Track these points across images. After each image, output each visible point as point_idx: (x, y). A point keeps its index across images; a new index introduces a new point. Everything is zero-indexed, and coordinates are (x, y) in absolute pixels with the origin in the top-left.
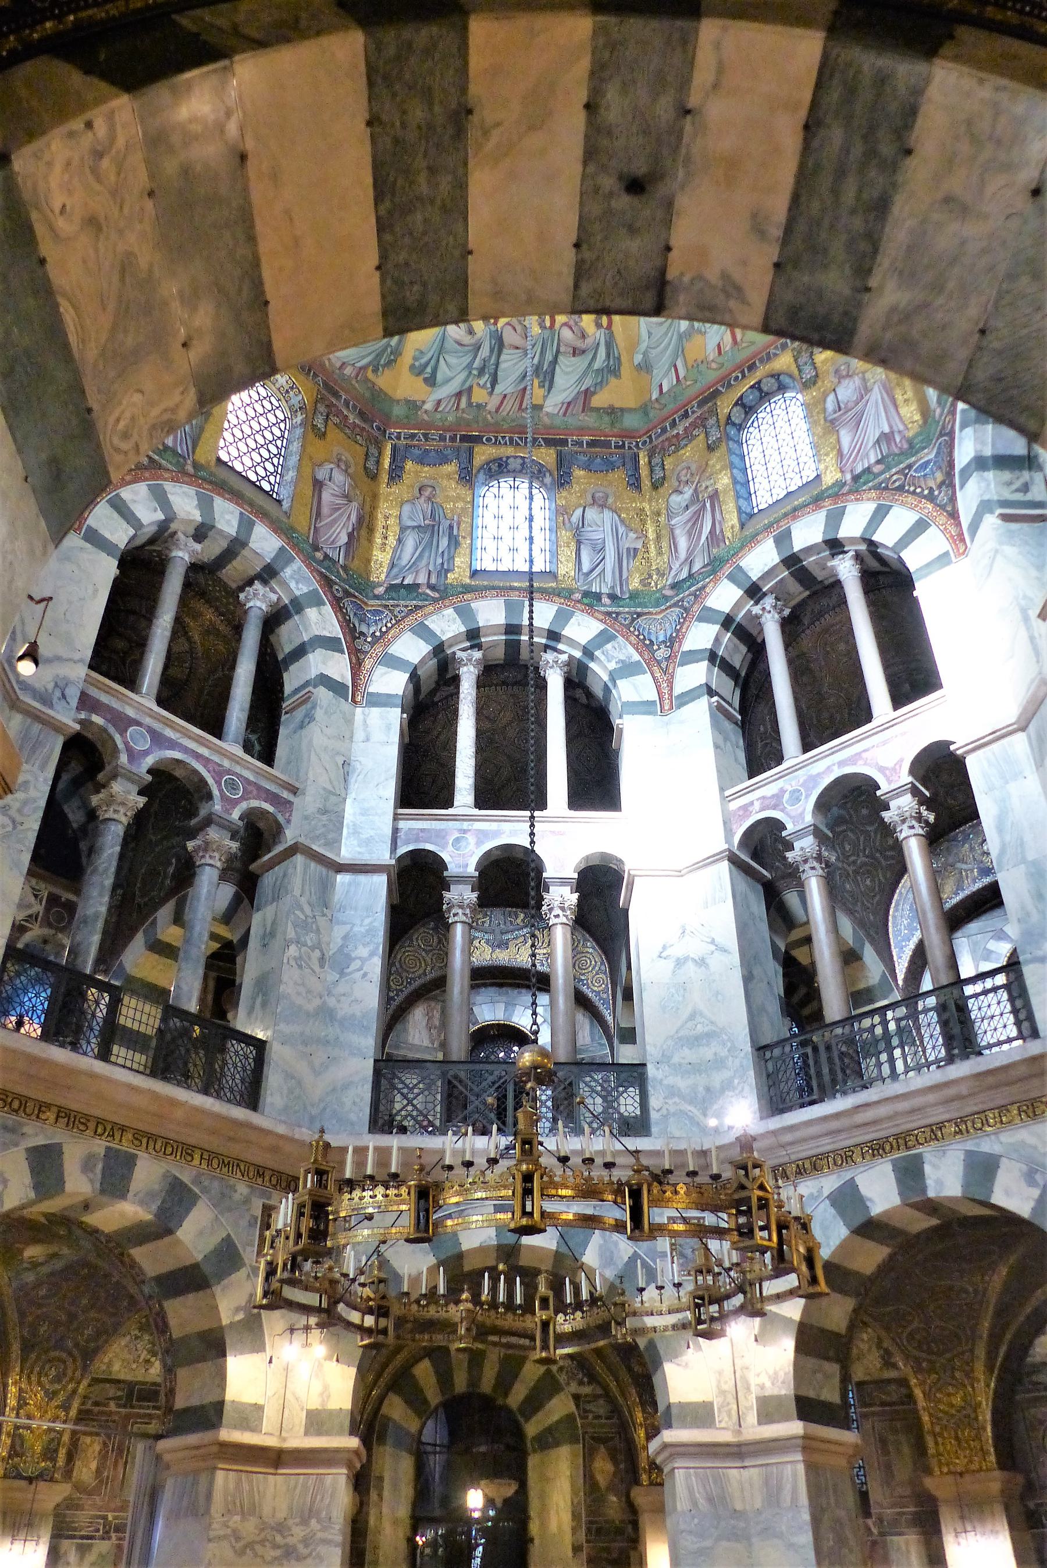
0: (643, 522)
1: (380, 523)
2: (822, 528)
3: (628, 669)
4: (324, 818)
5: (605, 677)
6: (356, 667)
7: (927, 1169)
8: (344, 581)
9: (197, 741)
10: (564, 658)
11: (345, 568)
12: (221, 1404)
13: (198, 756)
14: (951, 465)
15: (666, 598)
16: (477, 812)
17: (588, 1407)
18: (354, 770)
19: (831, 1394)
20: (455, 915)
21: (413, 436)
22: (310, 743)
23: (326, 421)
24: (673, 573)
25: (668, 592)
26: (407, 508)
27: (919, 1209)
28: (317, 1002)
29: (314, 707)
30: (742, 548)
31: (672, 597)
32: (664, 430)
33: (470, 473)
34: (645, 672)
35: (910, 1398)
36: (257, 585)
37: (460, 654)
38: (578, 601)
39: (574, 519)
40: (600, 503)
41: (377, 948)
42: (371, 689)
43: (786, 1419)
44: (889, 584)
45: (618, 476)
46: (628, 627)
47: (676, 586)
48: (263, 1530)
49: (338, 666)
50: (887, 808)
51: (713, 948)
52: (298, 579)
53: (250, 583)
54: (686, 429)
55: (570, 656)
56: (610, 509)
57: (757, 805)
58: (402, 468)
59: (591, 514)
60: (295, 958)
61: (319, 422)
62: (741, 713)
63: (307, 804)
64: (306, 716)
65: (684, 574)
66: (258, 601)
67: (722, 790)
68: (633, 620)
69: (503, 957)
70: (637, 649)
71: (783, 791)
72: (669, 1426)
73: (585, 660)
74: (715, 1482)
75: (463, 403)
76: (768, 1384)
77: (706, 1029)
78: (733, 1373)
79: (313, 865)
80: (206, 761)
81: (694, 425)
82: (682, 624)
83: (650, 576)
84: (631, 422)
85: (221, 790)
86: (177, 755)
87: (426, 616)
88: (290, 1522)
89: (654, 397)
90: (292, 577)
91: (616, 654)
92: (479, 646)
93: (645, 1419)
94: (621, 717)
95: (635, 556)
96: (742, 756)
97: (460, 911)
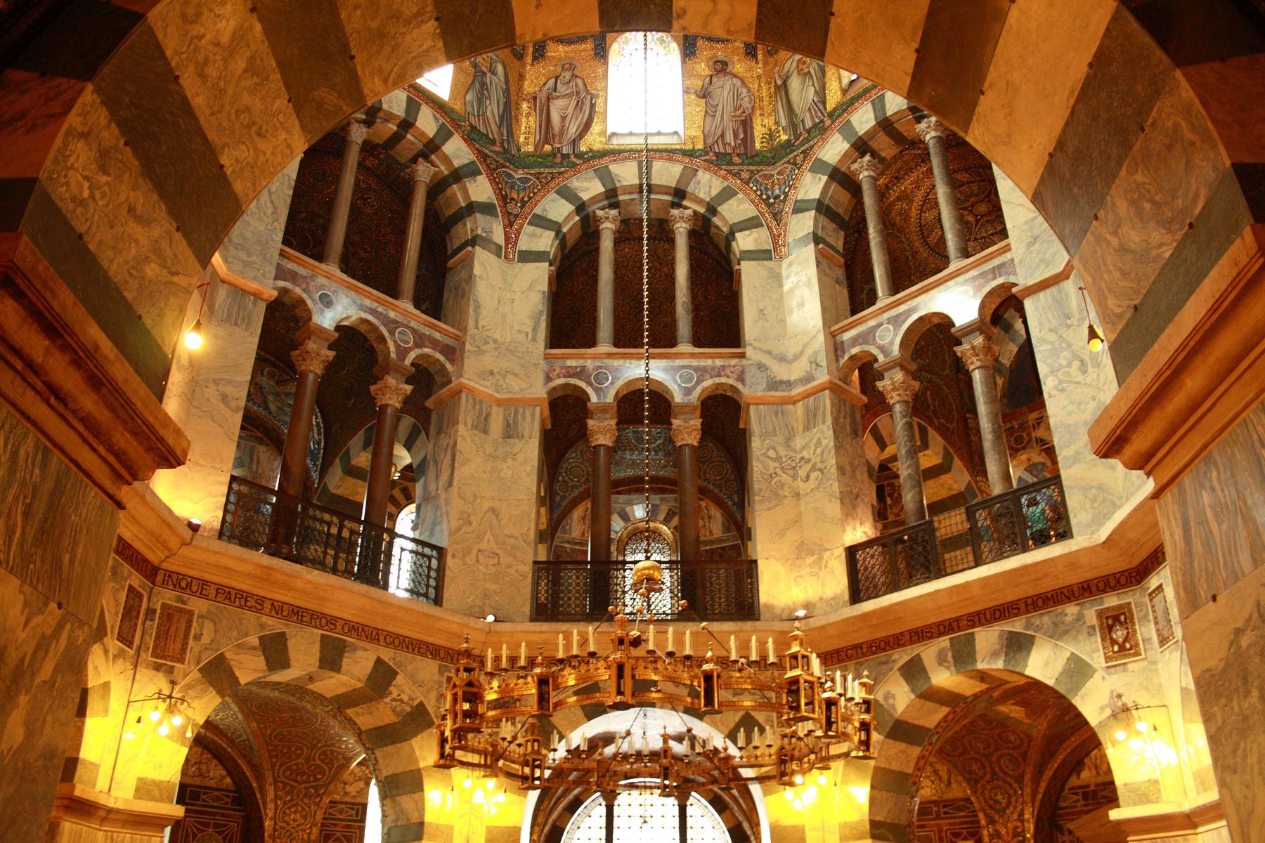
4: (1036, 247)
60: (1055, 388)
79: (1041, 295)
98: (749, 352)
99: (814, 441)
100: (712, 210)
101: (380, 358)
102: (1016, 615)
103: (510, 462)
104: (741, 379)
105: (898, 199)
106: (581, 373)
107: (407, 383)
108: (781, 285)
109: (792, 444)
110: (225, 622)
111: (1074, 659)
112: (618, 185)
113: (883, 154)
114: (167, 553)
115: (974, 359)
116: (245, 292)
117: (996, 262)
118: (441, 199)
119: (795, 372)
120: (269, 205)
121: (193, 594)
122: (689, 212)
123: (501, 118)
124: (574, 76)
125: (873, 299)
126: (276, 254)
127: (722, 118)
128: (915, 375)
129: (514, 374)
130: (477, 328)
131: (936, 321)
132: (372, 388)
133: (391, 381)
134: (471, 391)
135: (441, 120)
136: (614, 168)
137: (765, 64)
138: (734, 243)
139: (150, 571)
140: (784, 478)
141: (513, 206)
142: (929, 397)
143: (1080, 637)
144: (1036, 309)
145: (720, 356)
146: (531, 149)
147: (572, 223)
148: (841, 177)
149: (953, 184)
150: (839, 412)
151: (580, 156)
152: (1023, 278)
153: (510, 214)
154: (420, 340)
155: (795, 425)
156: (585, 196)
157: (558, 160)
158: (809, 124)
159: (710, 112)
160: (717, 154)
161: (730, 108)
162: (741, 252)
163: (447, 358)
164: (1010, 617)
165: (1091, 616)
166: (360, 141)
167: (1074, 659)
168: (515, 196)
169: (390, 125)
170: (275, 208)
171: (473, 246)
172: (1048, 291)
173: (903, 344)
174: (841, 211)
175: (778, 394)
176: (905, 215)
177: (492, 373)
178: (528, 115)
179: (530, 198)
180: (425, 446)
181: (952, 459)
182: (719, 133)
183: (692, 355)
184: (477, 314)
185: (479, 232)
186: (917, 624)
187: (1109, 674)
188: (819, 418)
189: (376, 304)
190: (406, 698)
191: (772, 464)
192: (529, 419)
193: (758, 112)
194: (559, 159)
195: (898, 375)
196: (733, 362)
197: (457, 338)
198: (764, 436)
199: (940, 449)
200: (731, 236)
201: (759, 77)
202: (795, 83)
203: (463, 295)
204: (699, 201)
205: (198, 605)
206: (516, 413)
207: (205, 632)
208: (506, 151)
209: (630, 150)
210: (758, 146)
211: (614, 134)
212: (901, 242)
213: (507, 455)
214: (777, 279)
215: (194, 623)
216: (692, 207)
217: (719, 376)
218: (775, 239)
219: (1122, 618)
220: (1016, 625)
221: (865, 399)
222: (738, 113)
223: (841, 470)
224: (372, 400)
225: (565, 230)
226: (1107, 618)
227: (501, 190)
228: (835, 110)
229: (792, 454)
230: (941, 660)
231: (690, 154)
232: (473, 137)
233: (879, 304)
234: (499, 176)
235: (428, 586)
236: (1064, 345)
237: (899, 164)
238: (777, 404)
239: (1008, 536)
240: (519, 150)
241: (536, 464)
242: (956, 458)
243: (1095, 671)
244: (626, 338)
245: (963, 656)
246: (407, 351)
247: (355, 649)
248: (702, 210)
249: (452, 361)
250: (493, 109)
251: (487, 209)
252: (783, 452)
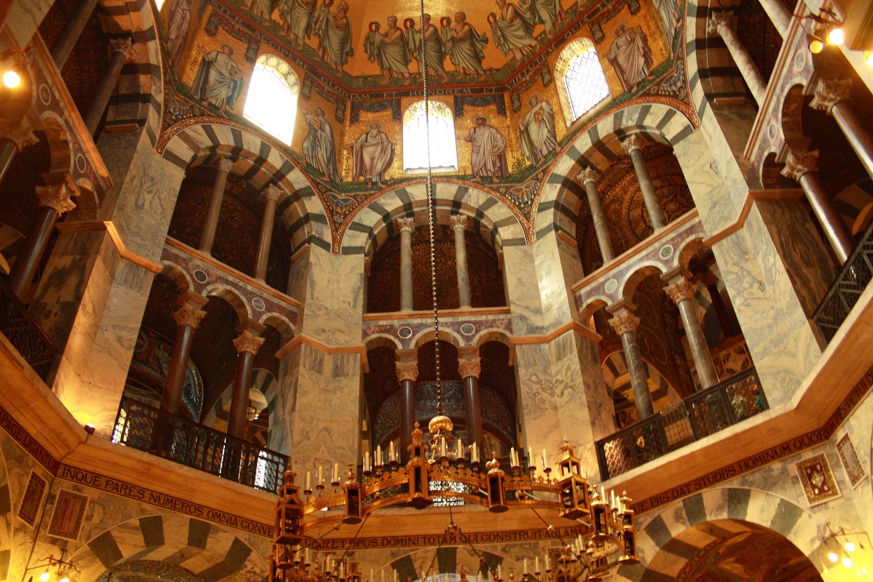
4: (717, 209)
11: (651, 73)
28: (772, 313)
60: (743, 304)
79: (724, 241)
80: (641, 260)
90: (627, 121)
98: (513, 308)
99: (565, 367)
100: (480, 214)
101: (241, 320)
102: (733, 475)
103: (338, 393)
104: (509, 327)
105: (612, 202)
106: (390, 329)
107: (261, 336)
108: (533, 262)
109: (549, 371)
110: (112, 507)
111: (784, 503)
112: (412, 200)
113: (599, 167)
114: (67, 451)
115: (679, 295)
116: (138, 265)
117: (688, 225)
118: (286, 213)
119: (547, 320)
120: (159, 207)
121: (87, 484)
122: (464, 217)
123: (329, 160)
124: (379, 132)
125: (599, 262)
126: (163, 242)
127: (484, 154)
128: (636, 313)
129: (340, 331)
130: (312, 298)
131: (648, 273)
132: (235, 341)
133: (248, 334)
134: (308, 342)
135: (286, 158)
136: (409, 189)
137: (512, 118)
138: (497, 236)
139: (54, 466)
140: (545, 395)
141: (339, 217)
142: (646, 342)
143: (787, 486)
144: (722, 251)
145: (491, 313)
146: (350, 179)
147: (380, 228)
148: (570, 185)
149: (650, 179)
150: (582, 346)
151: (385, 183)
152: (709, 232)
153: (335, 223)
154: (270, 307)
155: (550, 357)
156: (389, 209)
157: (370, 186)
158: (545, 152)
159: (475, 150)
160: (481, 177)
161: (489, 147)
162: (503, 241)
163: (291, 320)
165: (793, 468)
166: (228, 171)
167: (784, 503)
168: (339, 210)
169: (249, 161)
170: (164, 209)
171: (309, 243)
172: (729, 238)
173: (625, 292)
174: (572, 209)
175: (536, 336)
176: (618, 213)
177: (324, 331)
178: (348, 158)
179: (350, 212)
180: (276, 387)
181: (667, 386)
182: (483, 164)
183: (471, 313)
184: (312, 289)
185: (314, 233)
186: (656, 492)
187: (814, 512)
188: (568, 350)
189: (237, 280)
190: (258, 571)
191: (535, 386)
192: (352, 362)
193: (509, 149)
194: (370, 186)
195: (624, 313)
196: (502, 317)
197: (298, 306)
198: (528, 366)
199: (658, 379)
200: (495, 231)
201: (508, 127)
202: (533, 128)
203: (302, 277)
204: (471, 209)
205: (90, 493)
206: (343, 358)
207: (95, 514)
208: (332, 181)
209: (421, 177)
210: (510, 170)
211: (408, 169)
212: (617, 233)
213: (336, 388)
214: (530, 258)
215: (87, 507)
216: (465, 213)
217: (492, 326)
218: (526, 231)
219: (818, 467)
220: (735, 483)
221: (600, 337)
222: (495, 150)
223: (587, 386)
224: (234, 349)
225: (375, 232)
226: (806, 469)
227: (329, 206)
228: (562, 140)
229: (549, 378)
230: (678, 518)
231: (463, 178)
232: (308, 170)
233: (606, 266)
234: (328, 196)
235: (276, 485)
236: (745, 273)
237: (611, 175)
238: (536, 344)
239: (719, 418)
240: (342, 180)
241: (358, 394)
242: (670, 386)
243: (802, 511)
244: (421, 303)
245: (695, 511)
246: (261, 314)
247: (217, 531)
248: (473, 215)
249: (294, 323)
250: (323, 154)
251: (319, 218)
252: (542, 377)
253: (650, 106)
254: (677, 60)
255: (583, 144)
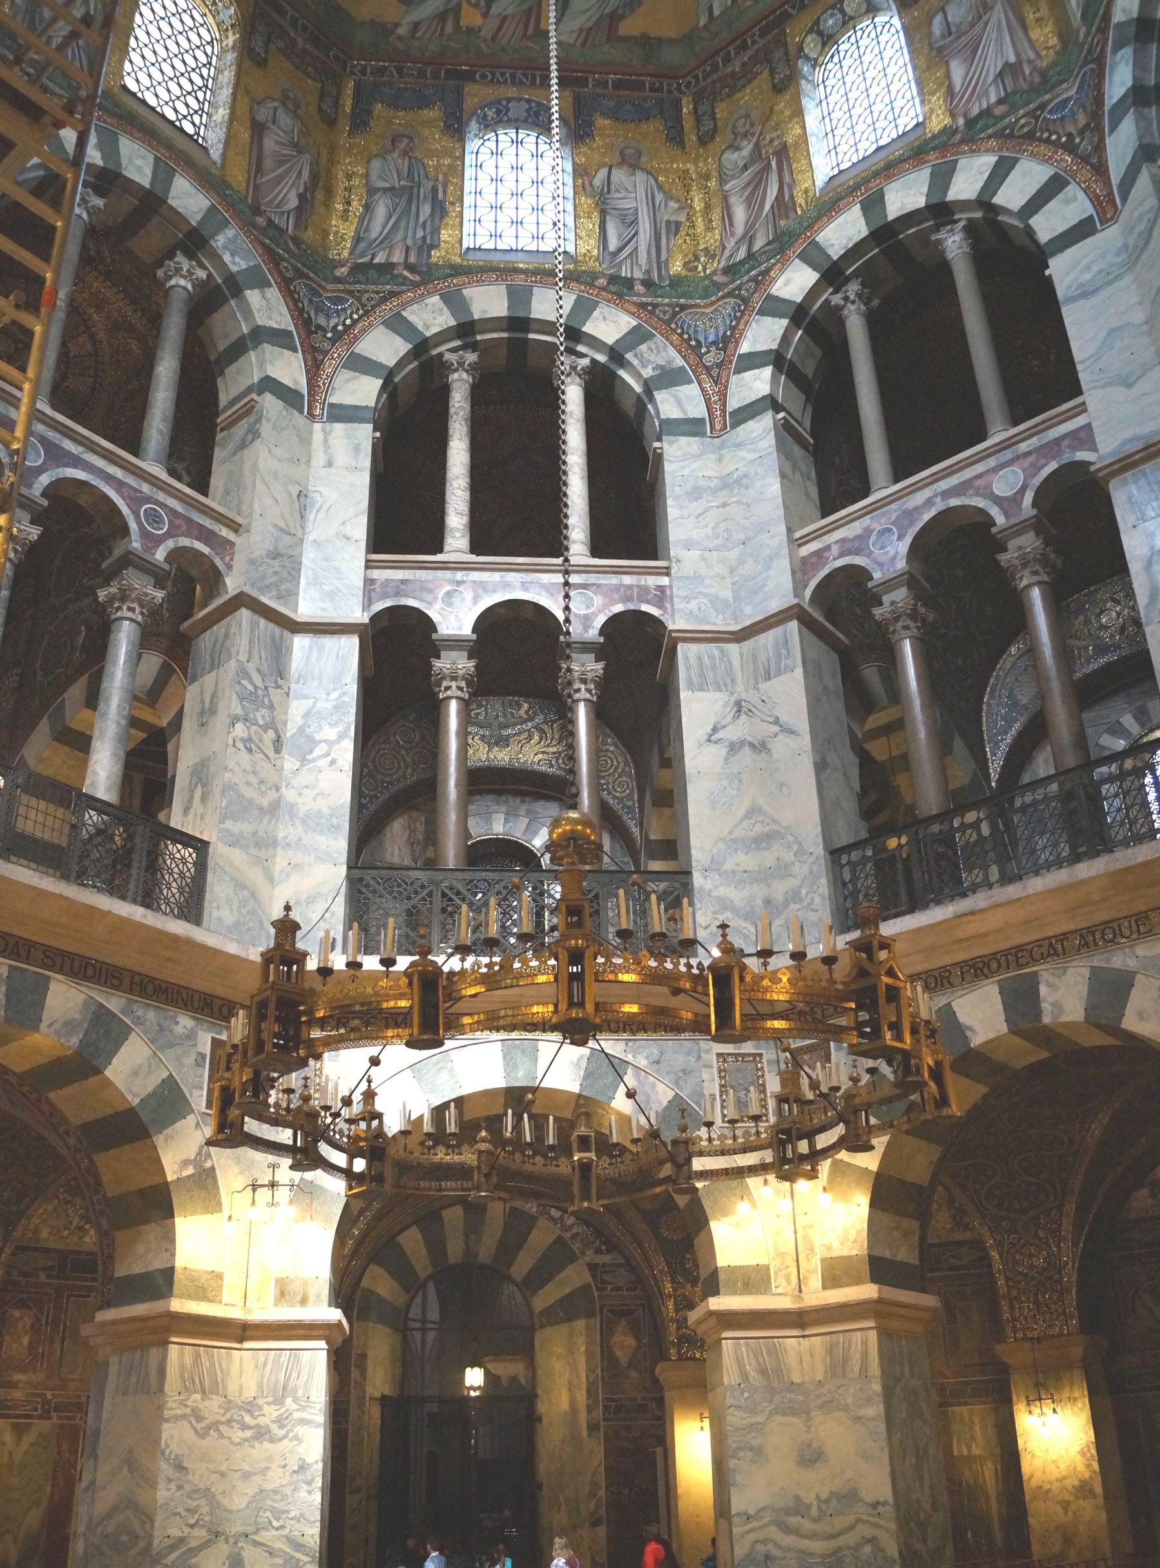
0: (687, 188)
1: (341, 184)
2: (925, 189)
3: (669, 378)
4: (276, 563)
5: (638, 389)
6: (313, 370)
7: (1043, 990)
8: (293, 256)
9: (104, 457)
10: (585, 362)
12: (171, 1270)
13: (108, 478)
14: (1099, 100)
15: (719, 286)
16: (474, 558)
17: (607, 1277)
18: (313, 504)
19: (907, 1254)
20: (447, 688)
21: (381, 71)
22: (255, 468)
23: (267, 43)
24: (727, 253)
25: (719, 279)
26: (376, 164)
27: (1025, 1039)
28: (272, 795)
29: (259, 420)
30: (818, 218)
31: (727, 284)
32: (715, 68)
33: (459, 120)
34: (690, 382)
35: (986, 1260)
36: (180, 258)
37: (448, 356)
38: (604, 289)
39: (597, 182)
40: (631, 162)
41: (349, 728)
42: (333, 399)
43: (858, 1281)
44: (1013, 263)
45: (654, 127)
46: (667, 323)
47: (731, 270)
48: (228, 1409)
49: (289, 368)
50: (1004, 549)
51: (776, 728)
52: (234, 251)
53: (171, 255)
54: (744, 64)
55: (593, 361)
56: (643, 170)
57: (835, 550)
58: (369, 112)
59: (619, 175)
60: (243, 740)
61: (258, 44)
62: (812, 436)
63: (255, 542)
64: (249, 431)
65: (742, 254)
66: (183, 279)
67: (790, 531)
68: (675, 314)
69: (502, 757)
70: (680, 352)
71: (868, 531)
72: (716, 1293)
73: (613, 366)
74: (769, 1352)
75: (449, 28)
76: (836, 1245)
77: (767, 829)
78: (790, 1232)
79: (263, 622)
80: (119, 485)
81: (755, 60)
82: (738, 319)
83: (697, 259)
84: (673, 57)
85: (139, 523)
86: (81, 475)
87: (404, 306)
88: (260, 1401)
89: (703, 21)
90: (225, 247)
91: (652, 358)
92: (474, 346)
93: (675, 1290)
94: (659, 439)
95: (677, 232)
96: (814, 492)
97: (454, 684)
102: (114, 987)
164: (105, 985)
165: (205, 1041)
172: (271, 625)
220: (114, 1003)
253: (270, 286)
254: (350, 293)
255: (138, 164)
